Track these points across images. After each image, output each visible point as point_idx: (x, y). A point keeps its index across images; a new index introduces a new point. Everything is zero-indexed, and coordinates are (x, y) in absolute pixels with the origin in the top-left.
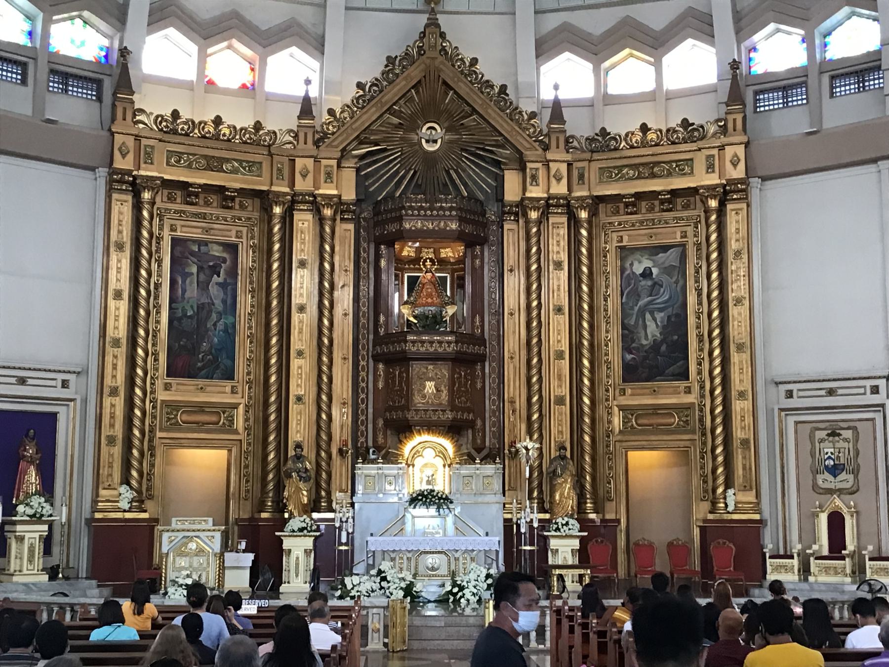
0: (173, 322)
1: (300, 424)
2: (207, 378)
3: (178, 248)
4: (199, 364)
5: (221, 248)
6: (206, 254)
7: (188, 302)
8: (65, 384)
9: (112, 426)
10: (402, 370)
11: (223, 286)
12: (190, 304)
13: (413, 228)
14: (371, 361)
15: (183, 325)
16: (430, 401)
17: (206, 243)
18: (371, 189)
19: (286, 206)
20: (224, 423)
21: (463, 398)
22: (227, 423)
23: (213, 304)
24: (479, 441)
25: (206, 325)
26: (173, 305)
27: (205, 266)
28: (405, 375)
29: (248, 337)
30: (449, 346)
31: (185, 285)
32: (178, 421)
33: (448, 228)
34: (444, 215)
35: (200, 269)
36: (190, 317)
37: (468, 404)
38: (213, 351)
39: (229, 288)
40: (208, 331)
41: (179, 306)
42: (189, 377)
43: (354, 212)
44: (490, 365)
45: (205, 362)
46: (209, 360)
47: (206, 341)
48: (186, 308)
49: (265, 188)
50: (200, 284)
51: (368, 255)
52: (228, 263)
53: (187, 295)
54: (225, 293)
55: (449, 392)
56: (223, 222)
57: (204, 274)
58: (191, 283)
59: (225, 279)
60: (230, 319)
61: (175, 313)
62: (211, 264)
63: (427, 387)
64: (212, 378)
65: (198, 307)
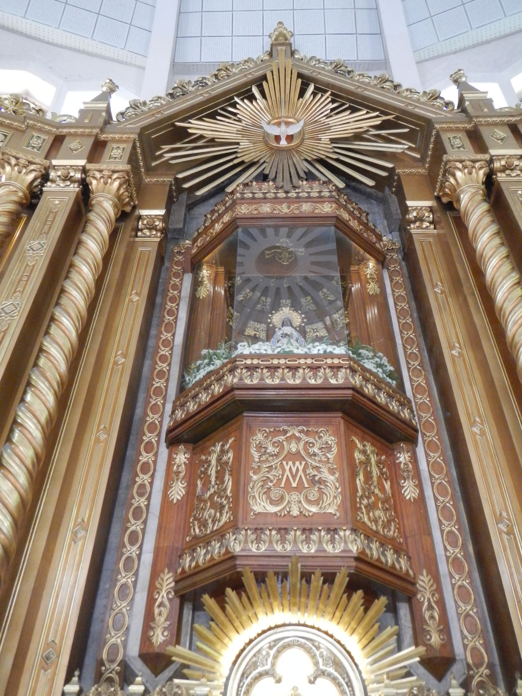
10: (228, 445)
13: (255, 212)
14: (164, 451)
16: (295, 512)
18: (186, 186)
21: (378, 513)
24: (435, 639)
28: (231, 455)
30: (335, 376)
33: (317, 211)
34: (309, 197)
37: (392, 532)
44: (427, 455)
51: (180, 292)
55: (342, 484)
63: (287, 473)
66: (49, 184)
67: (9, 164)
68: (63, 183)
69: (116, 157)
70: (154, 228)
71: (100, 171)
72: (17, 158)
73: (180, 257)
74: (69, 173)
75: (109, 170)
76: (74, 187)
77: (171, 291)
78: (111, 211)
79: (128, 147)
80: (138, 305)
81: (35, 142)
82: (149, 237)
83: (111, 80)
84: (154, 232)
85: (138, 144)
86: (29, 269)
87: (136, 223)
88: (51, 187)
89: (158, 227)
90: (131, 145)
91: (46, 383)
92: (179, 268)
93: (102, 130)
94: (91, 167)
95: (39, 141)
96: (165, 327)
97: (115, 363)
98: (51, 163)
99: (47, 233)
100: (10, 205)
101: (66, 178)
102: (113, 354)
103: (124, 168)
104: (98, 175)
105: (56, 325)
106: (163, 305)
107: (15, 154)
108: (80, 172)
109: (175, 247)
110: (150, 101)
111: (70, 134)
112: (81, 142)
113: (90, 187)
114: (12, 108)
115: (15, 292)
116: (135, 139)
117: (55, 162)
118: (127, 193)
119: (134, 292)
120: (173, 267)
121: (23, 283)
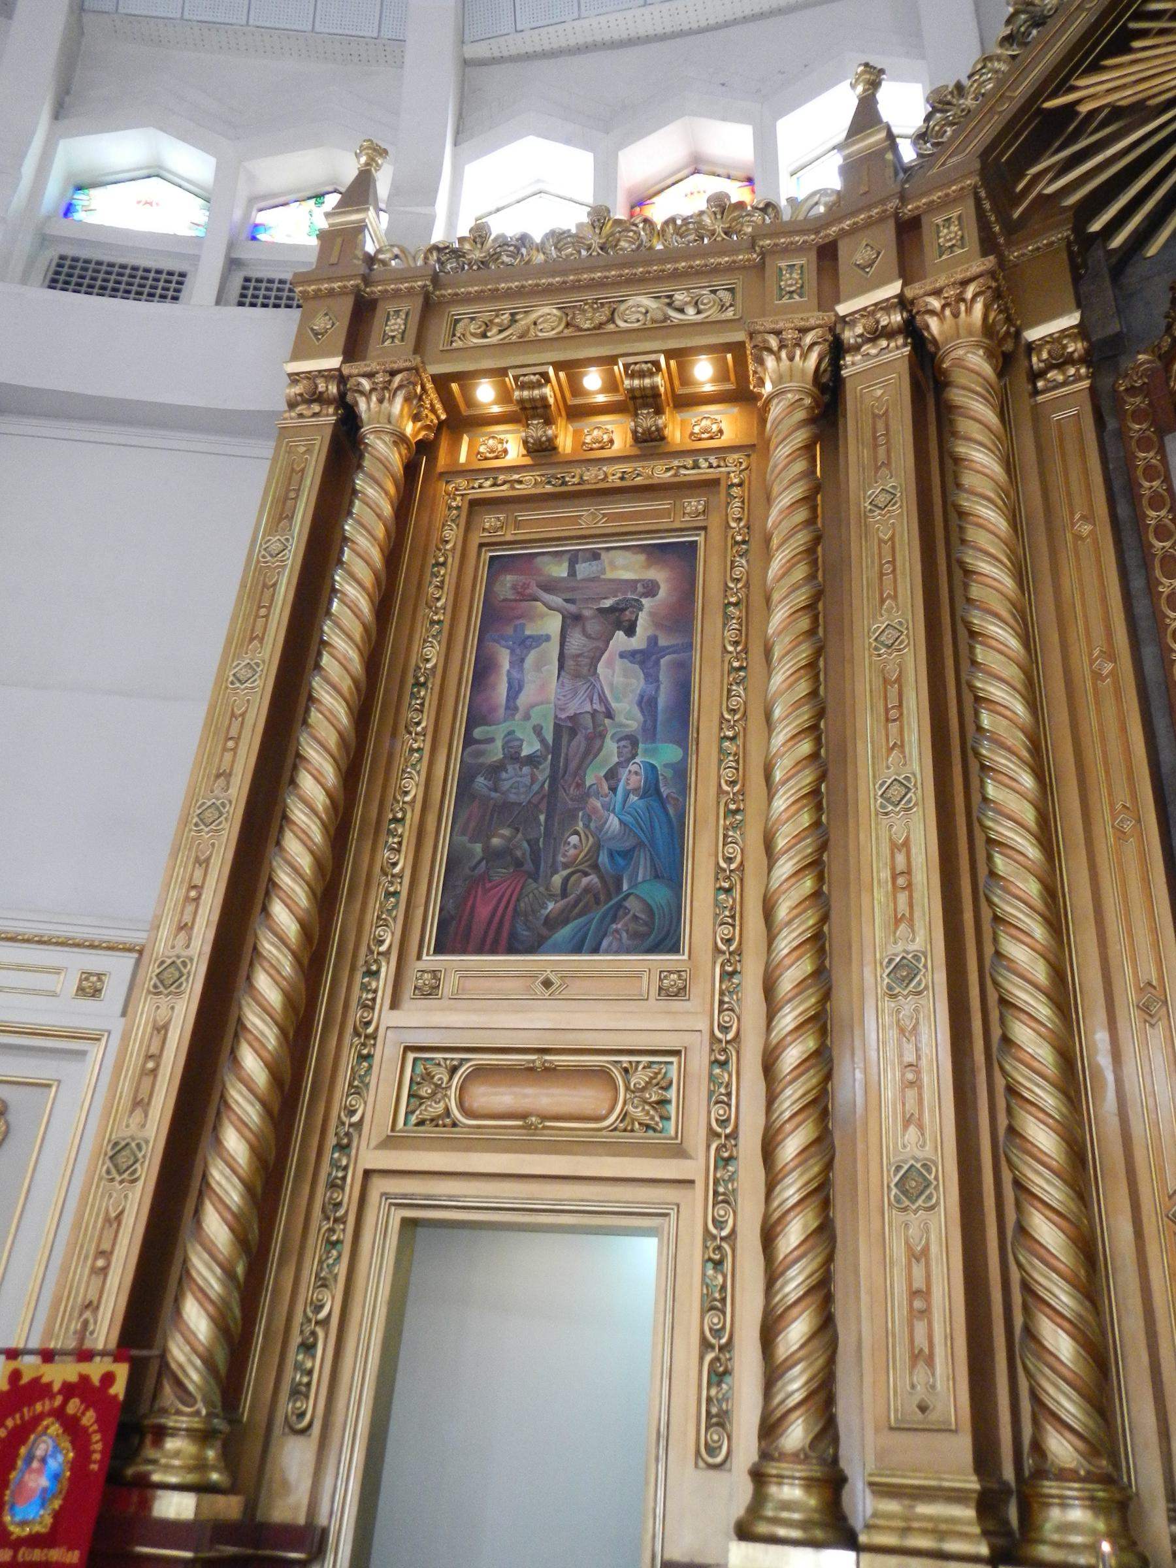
0: (472, 778)
1: (916, 1084)
2: (578, 949)
3: (509, 579)
4: (551, 906)
5: (641, 558)
6: (592, 580)
7: (527, 717)
8: (91, 988)
9: (140, 1103)
11: (645, 659)
12: (529, 725)
15: (506, 785)
17: (595, 555)
19: (813, 358)
20: (624, 1116)
22: (637, 1112)
23: (609, 715)
25: (583, 779)
26: (478, 732)
27: (587, 613)
29: (720, 790)
31: (521, 670)
32: (447, 1112)
35: (572, 620)
36: (532, 760)
38: (603, 858)
39: (663, 661)
40: (588, 795)
41: (499, 732)
42: (511, 950)
43: (1086, 360)
45: (571, 898)
46: (587, 890)
47: (580, 827)
48: (519, 734)
49: (740, 336)
50: (570, 663)
52: (662, 593)
53: (523, 700)
54: (652, 677)
56: (639, 480)
57: (584, 633)
58: (539, 666)
59: (653, 640)
60: (668, 753)
61: (481, 753)
62: (607, 603)
64: (595, 950)
65: (558, 728)
66: (849, 359)
67: (770, 350)
68: (874, 347)
69: (953, 245)
70: (1069, 360)
71: (937, 293)
72: (778, 333)
73: (1138, 400)
74: (878, 322)
75: (954, 284)
76: (897, 348)
77: (1147, 484)
78: (987, 369)
79: (966, 209)
80: (1096, 542)
81: (789, 282)
82: (1065, 383)
83: (866, 65)
84: (1072, 371)
85: (983, 194)
86: (886, 548)
87: (1026, 363)
88: (853, 364)
89: (1076, 355)
90: (971, 202)
91: (1014, 759)
92: (1144, 426)
93: (903, 198)
94: (917, 292)
95: (795, 276)
96: (1161, 567)
97: (1097, 676)
98: (837, 315)
99: (887, 464)
100: (798, 433)
101: (876, 334)
102: (1086, 660)
103: (983, 268)
104: (936, 303)
105: (981, 643)
106: (1138, 518)
107: (772, 326)
108: (898, 310)
109: (1118, 379)
110: (970, 77)
111: (843, 233)
112: (871, 243)
113: (926, 334)
114: (719, 227)
115: (882, 601)
116: (975, 187)
117: (843, 309)
118: (1001, 316)
119: (1077, 516)
120: (1130, 429)
121: (888, 579)
